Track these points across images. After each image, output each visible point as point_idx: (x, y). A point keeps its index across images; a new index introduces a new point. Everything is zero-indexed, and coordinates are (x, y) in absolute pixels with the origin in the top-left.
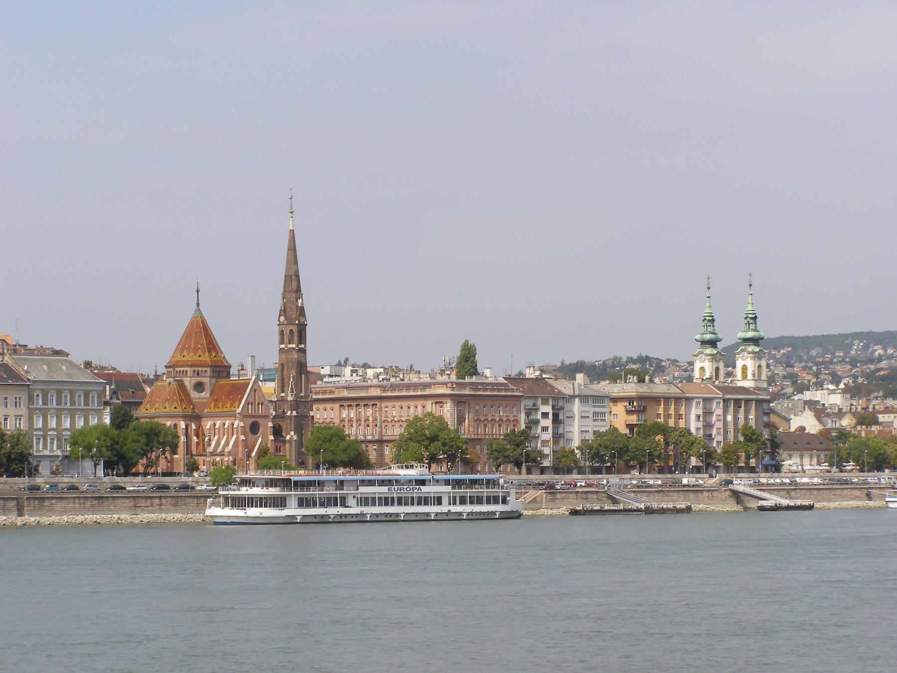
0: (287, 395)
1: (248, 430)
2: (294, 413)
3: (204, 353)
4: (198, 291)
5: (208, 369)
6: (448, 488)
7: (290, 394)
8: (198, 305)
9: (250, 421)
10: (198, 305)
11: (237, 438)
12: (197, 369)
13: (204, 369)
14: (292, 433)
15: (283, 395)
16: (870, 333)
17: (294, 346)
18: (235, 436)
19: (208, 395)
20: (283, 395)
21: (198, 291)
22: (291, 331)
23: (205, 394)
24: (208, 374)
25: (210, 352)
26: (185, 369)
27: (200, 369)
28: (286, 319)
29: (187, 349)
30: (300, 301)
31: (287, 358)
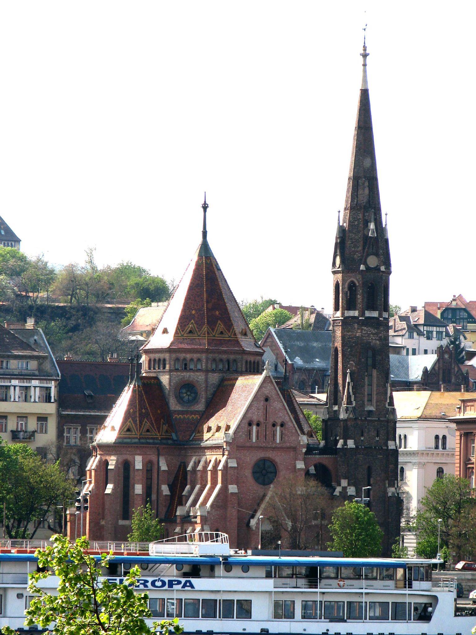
0: (339, 408)
1: (248, 473)
2: (351, 444)
3: (200, 325)
4: (205, 207)
6: (269, 584)
8: (205, 234)
9: (251, 458)
10: (205, 234)
15: (336, 408)
16: (387, 241)
17: (356, 313)
18: (219, 486)
20: (336, 408)
21: (205, 207)
25: (212, 323)
26: (161, 356)
27: (188, 356)
28: (343, 261)
30: (372, 226)
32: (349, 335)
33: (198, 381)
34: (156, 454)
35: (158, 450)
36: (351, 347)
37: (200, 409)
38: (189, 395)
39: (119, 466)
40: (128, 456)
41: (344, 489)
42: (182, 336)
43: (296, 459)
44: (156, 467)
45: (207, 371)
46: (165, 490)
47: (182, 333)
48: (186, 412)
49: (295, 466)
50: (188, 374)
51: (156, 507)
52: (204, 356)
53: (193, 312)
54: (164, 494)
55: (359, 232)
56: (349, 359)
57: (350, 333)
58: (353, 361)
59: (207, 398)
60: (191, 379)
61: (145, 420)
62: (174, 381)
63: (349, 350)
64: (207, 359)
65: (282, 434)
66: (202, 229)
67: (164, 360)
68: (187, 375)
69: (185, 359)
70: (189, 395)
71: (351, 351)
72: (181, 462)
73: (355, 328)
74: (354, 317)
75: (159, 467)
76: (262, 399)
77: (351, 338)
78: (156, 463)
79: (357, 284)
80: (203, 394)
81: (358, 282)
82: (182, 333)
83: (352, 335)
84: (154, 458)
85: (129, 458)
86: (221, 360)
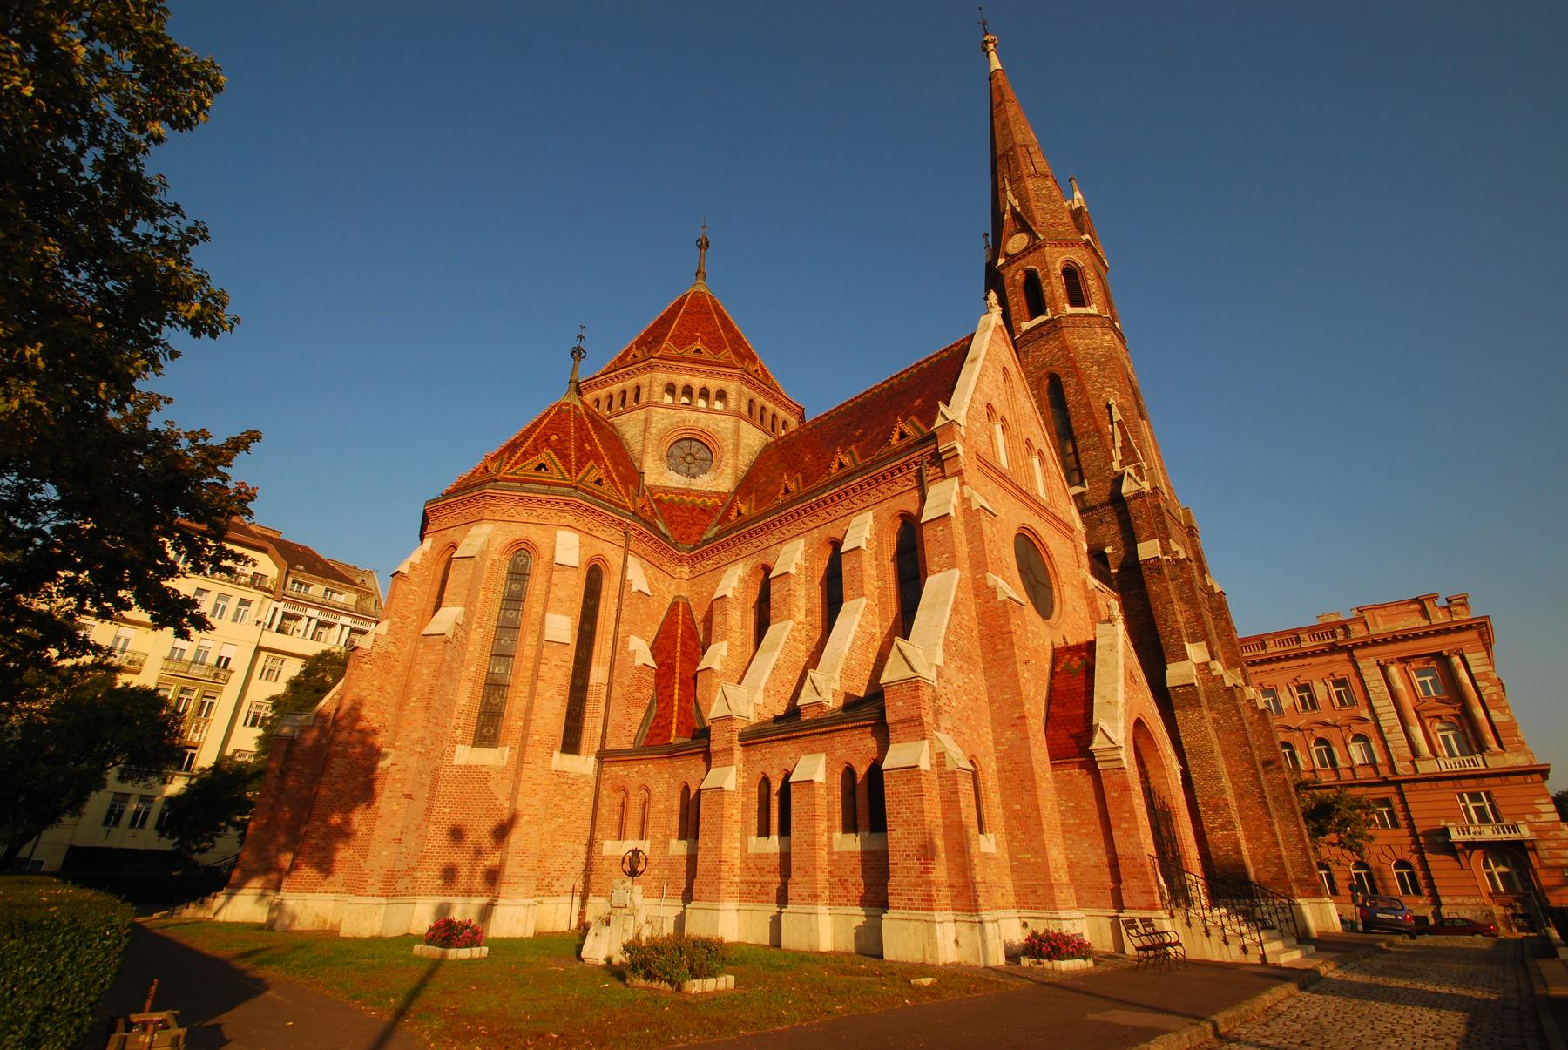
17: (1093, 309)
34: (622, 544)
36: (1099, 364)
39: (496, 557)
40: (532, 528)
45: (740, 416)
46: (640, 651)
48: (687, 492)
49: (1084, 582)
50: (695, 414)
51: (602, 711)
52: (732, 387)
54: (639, 662)
59: (736, 467)
60: (701, 425)
61: (592, 462)
64: (740, 393)
67: (638, 388)
68: (690, 417)
69: (688, 391)
78: (617, 570)
79: (1081, 264)
80: (729, 457)
84: (613, 555)
85: (534, 534)
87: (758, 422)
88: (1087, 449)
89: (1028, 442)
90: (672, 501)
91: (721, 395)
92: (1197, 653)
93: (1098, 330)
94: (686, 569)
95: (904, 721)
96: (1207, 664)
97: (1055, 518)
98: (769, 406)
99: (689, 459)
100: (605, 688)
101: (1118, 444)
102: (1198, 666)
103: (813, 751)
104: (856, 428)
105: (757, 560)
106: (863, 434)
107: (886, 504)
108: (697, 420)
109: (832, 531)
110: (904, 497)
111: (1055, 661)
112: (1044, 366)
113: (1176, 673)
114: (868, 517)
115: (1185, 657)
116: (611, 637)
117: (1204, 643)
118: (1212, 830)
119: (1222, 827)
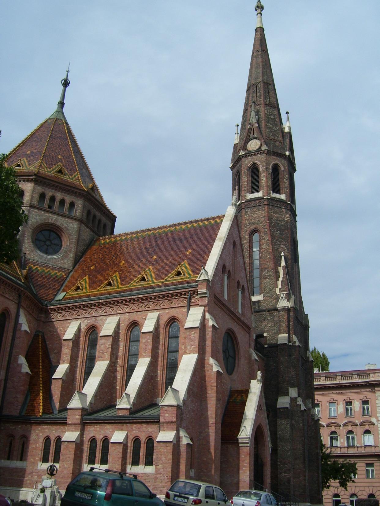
4: (66, 84)
5: (79, 203)
7: (283, 295)
8: (62, 104)
10: (62, 104)
11: (200, 366)
12: (49, 193)
13: (68, 199)
14: (293, 392)
17: (283, 197)
19: (68, 263)
21: (66, 84)
22: (276, 168)
23: (61, 260)
24: (78, 211)
27: (59, 196)
29: (28, 156)
31: (270, 218)
32: (277, 217)
33: (68, 230)
35: (20, 296)
36: (280, 230)
37: (66, 266)
38: (48, 246)
41: (294, 400)
42: (50, 172)
43: (250, 347)
44: (12, 323)
47: (50, 170)
49: (250, 355)
53: (60, 157)
55: (276, 125)
56: (280, 242)
57: (277, 215)
58: (285, 245)
60: (58, 224)
62: (34, 220)
63: (279, 232)
64: (84, 206)
65: (242, 304)
66: (59, 100)
70: (48, 246)
71: (281, 234)
72: (37, 331)
73: (283, 212)
74: (281, 201)
75: (17, 325)
76: (232, 241)
77: (279, 221)
78: (13, 316)
79: (283, 169)
81: (284, 167)
82: (50, 170)
83: (280, 217)
84: (12, 308)
86: (95, 216)
87: (90, 225)
88: (266, 278)
89: (238, 282)
90: (37, 270)
91: (72, 205)
92: (293, 392)
93: (284, 210)
94: (43, 316)
95: (166, 423)
96: (296, 398)
97: (243, 323)
98: (98, 214)
99: (48, 243)
100: (3, 382)
101: (281, 279)
102: (291, 399)
103: (122, 430)
104: (153, 254)
105: (90, 322)
106: (157, 260)
107: (167, 311)
108: (56, 220)
109: (135, 317)
110: (177, 310)
111: (230, 396)
112: (254, 224)
113: (283, 402)
114: (155, 315)
115: (287, 394)
116: (7, 354)
117: (296, 388)
118: (281, 473)
119: (285, 472)
